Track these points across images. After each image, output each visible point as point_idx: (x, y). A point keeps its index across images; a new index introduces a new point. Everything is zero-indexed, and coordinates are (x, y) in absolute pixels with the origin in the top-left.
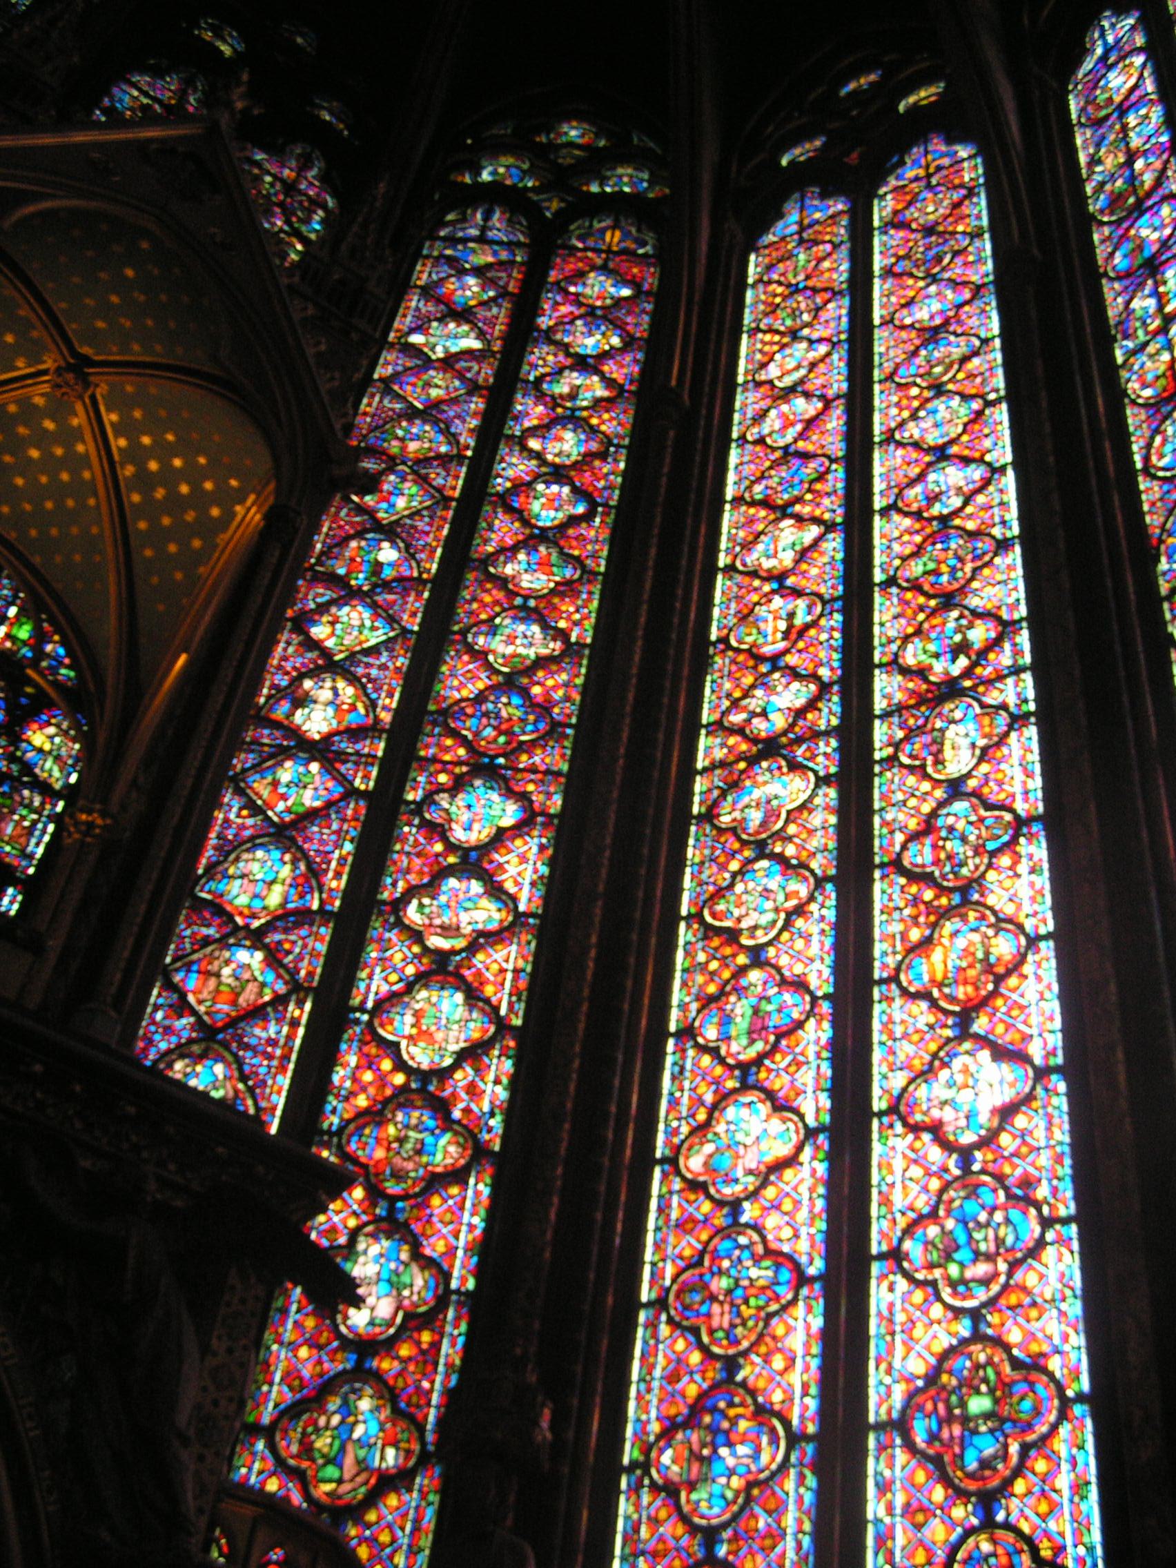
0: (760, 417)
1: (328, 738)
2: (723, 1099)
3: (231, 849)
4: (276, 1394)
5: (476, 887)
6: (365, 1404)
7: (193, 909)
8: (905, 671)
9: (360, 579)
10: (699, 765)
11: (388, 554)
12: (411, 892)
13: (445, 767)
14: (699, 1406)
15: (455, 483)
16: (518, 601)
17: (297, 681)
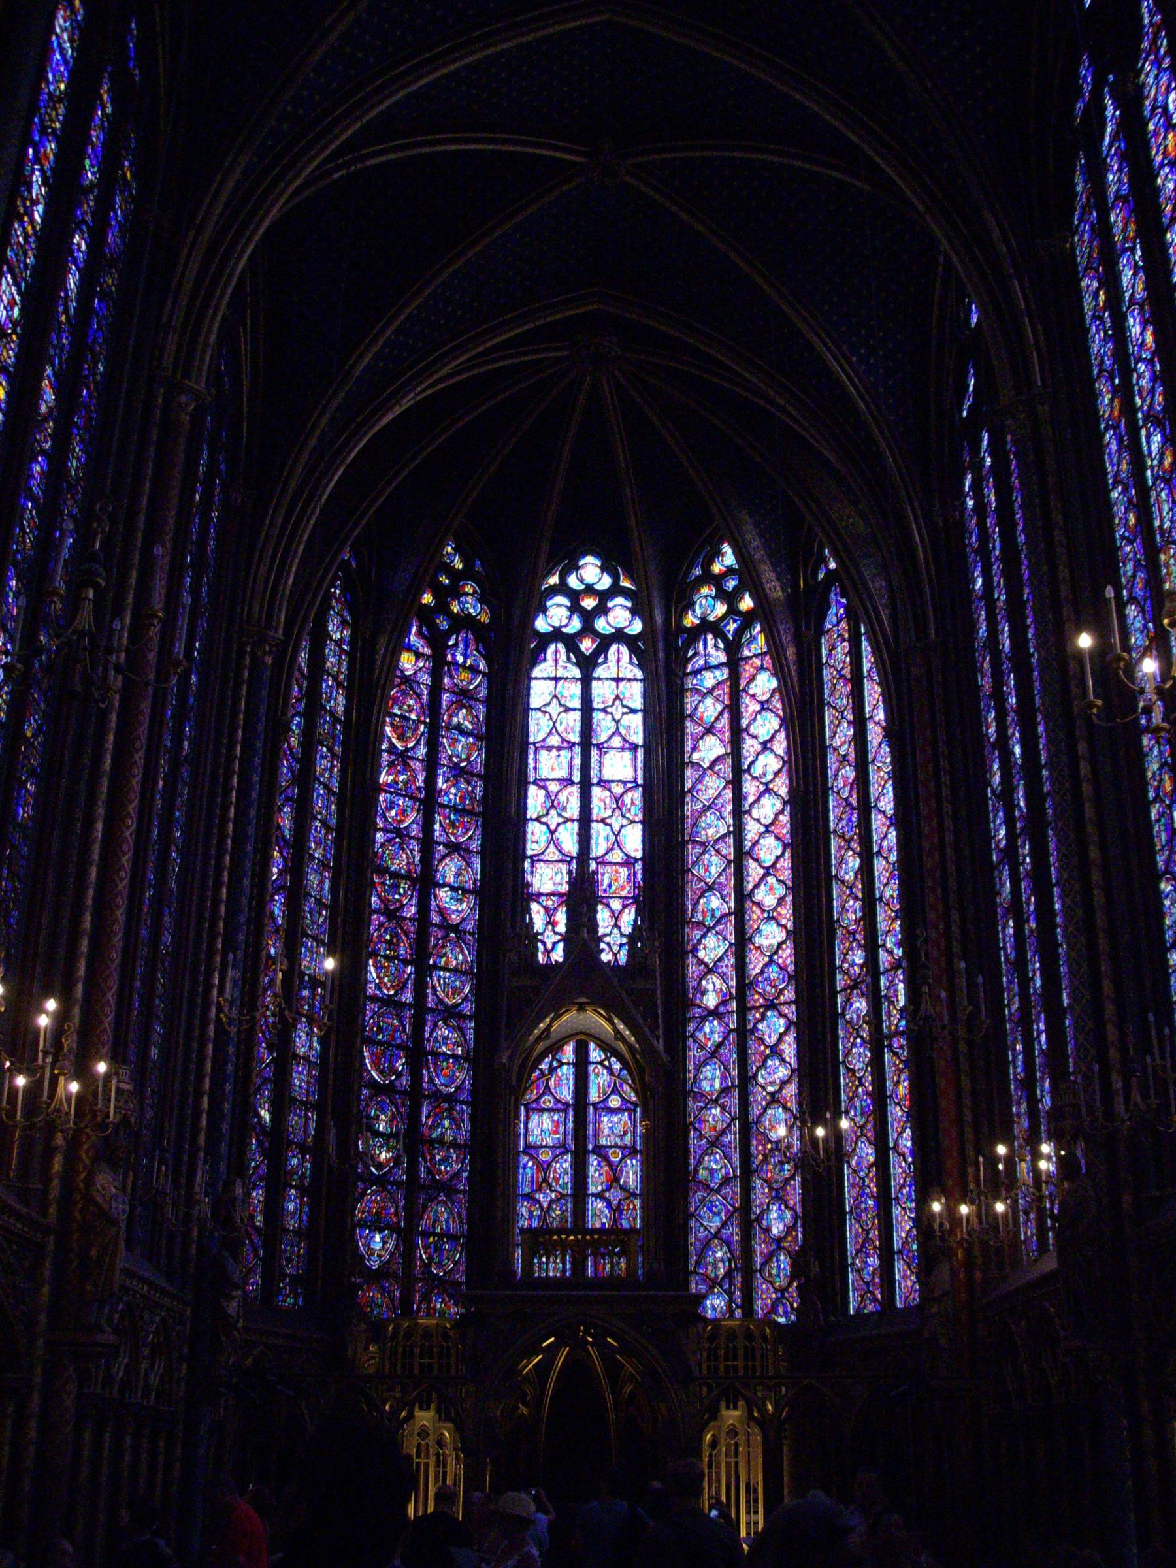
0: (836, 775)
1: (717, 1007)
2: (858, 1138)
3: (698, 1069)
4: (759, 1260)
5: (777, 1063)
6: (782, 1258)
7: (694, 1098)
8: (887, 951)
9: (709, 922)
10: (838, 989)
11: (715, 902)
12: (758, 1069)
13: (757, 1008)
14: (863, 1246)
15: (729, 851)
16: (766, 915)
17: (699, 983)
